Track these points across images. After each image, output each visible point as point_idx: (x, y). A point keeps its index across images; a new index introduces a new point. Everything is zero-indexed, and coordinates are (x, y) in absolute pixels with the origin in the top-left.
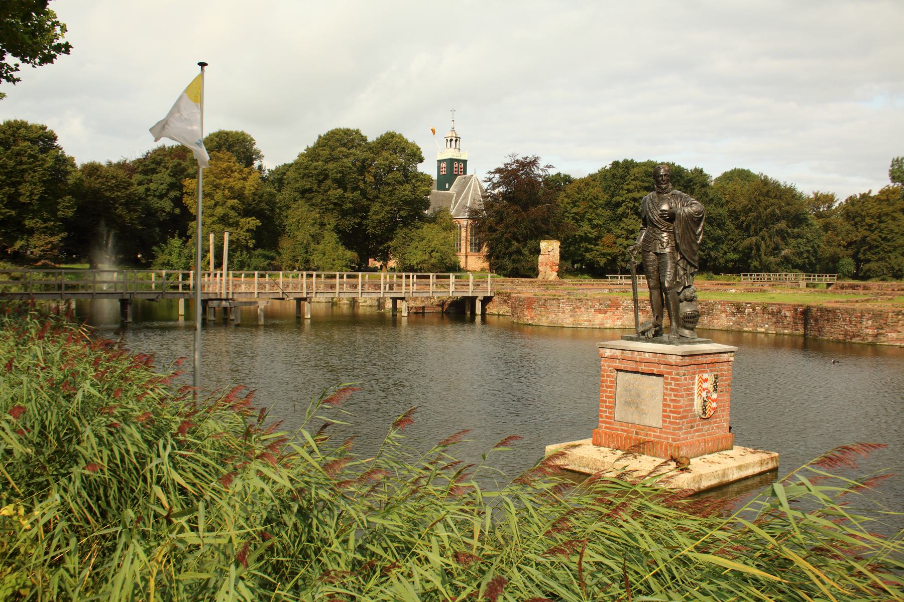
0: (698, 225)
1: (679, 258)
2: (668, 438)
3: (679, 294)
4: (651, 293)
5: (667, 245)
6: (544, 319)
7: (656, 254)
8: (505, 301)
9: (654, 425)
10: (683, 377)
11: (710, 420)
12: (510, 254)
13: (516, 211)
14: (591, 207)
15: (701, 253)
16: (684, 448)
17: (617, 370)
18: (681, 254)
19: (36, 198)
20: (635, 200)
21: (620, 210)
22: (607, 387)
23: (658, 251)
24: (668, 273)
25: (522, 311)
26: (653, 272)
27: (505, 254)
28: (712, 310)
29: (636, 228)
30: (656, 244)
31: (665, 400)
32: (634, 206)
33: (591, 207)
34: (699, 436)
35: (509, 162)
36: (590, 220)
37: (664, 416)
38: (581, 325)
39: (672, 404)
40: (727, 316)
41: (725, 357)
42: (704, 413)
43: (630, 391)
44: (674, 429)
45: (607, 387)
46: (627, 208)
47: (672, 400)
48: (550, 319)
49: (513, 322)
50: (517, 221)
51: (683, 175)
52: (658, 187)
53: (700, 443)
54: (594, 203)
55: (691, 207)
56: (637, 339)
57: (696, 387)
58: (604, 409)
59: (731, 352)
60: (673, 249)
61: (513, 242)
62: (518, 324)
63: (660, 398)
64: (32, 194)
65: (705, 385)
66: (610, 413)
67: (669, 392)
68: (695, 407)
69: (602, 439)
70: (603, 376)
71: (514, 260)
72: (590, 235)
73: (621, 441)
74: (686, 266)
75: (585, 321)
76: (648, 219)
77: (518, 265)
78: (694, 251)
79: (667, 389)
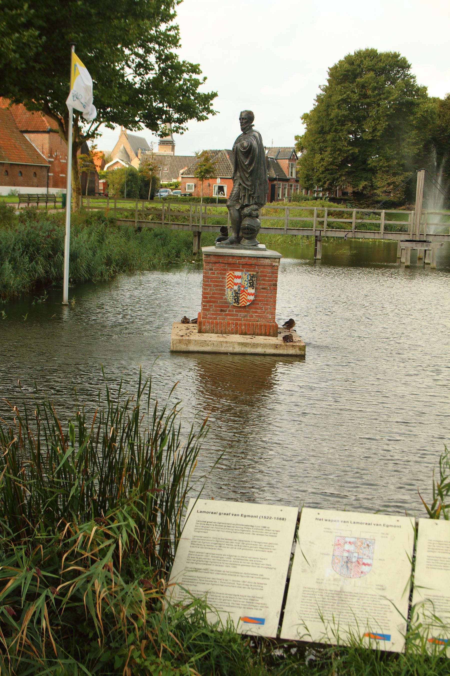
10: (210, 272)
19: (378, 134)
41: (267, 261)
64: (375, 130)
65: (238, 281)
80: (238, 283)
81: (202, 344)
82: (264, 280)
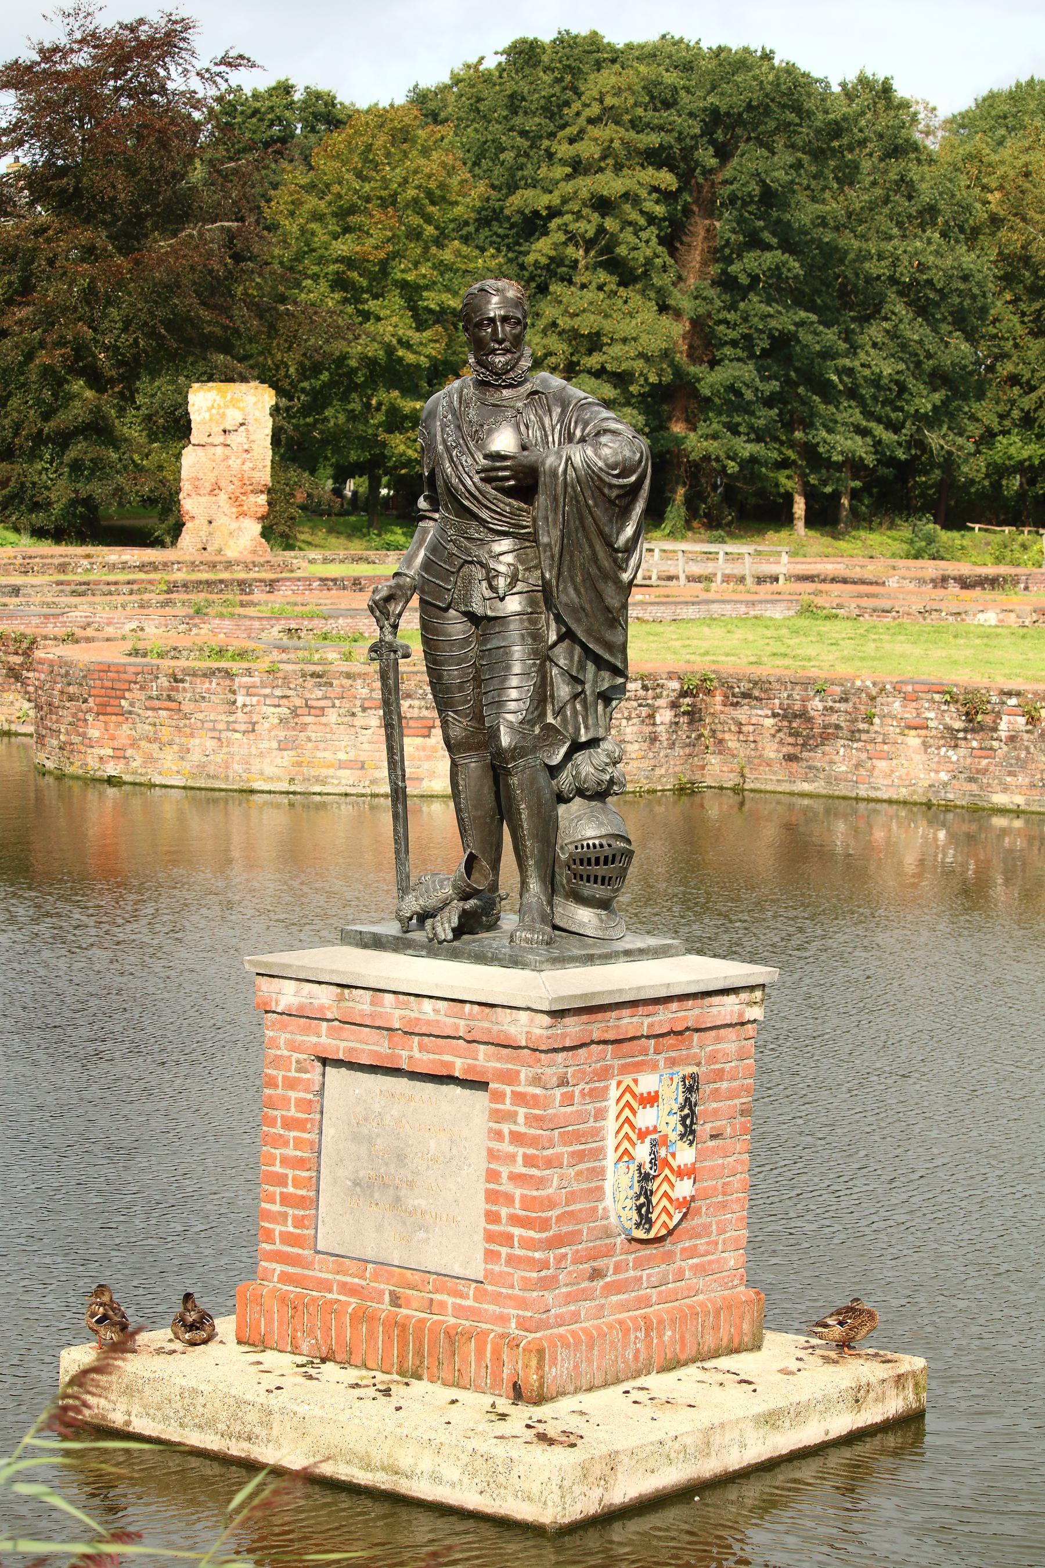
0: (624, 514)
1: (553, 637)
2: (503, 1319)
3: (553, 771)
4: (454, 765)
5: (512, 584)
6: (168, 759)
7: (473, 618)
8: (14, 674)
9: (457, 1271)
10: (558, 1093)
11: (668, 1245)
12: (63, 439)
13: (90, 252)
14: (415, 234)
15: (887, 436)
16: (561, 1353)
17: (324, 1061)
18: (558, 619)
20: (603, 205)
21: (541, 249)
22: (289, 1124)
23: (478, 608)
24: (514, 694)
25: (77, 723)
26: (461, 687)
27: (39, 438)
28: (869, 719)
29: (607, 325)
30: (469, 581)
31: (492, 1176)
32: (601, 230)
33: (415, 234)
34: (625, 1307)
35: (64, 41)
36: (411, 292)
37: (490, 1237)
38: (318, 780)
39: (518, 1193)
40: (926, 746)
42: (645, 1220)
43: (370, 1140)
44: (527, 1285)
45: (289, 1124)
46: (572, 238)
47: (514, 1178)
48: (196, 756)
49: (43, 772)
50: (89, 295)
51: (809, 105)
52: (479, 362)
53: (626, 1332)
54: (428, 219)
55: (597, 446)
56: (398, 945)
57: (611, 1124)
58: (276, 1208)
59: (752, 988)
60: (532, 602)
61: (77, 385)
62: (61, 777)
63: (479, 1164)
65: (646, 1118)
66: (299, 1223)
67: (507, 1147)
68: (608, 1202)
69: (269, 1322)
70: (272, 1083)
71: (76, 467)
72: (410, 358)
73: (340, 1327)
74: (582, 668)
75: (342, 765)
76: (440, 482)
77: (98, 489)
78: (608, 609)
79: (499, 1135)
80: (648, 1132)
81: (651, 1463)
82: (716, 1094)
